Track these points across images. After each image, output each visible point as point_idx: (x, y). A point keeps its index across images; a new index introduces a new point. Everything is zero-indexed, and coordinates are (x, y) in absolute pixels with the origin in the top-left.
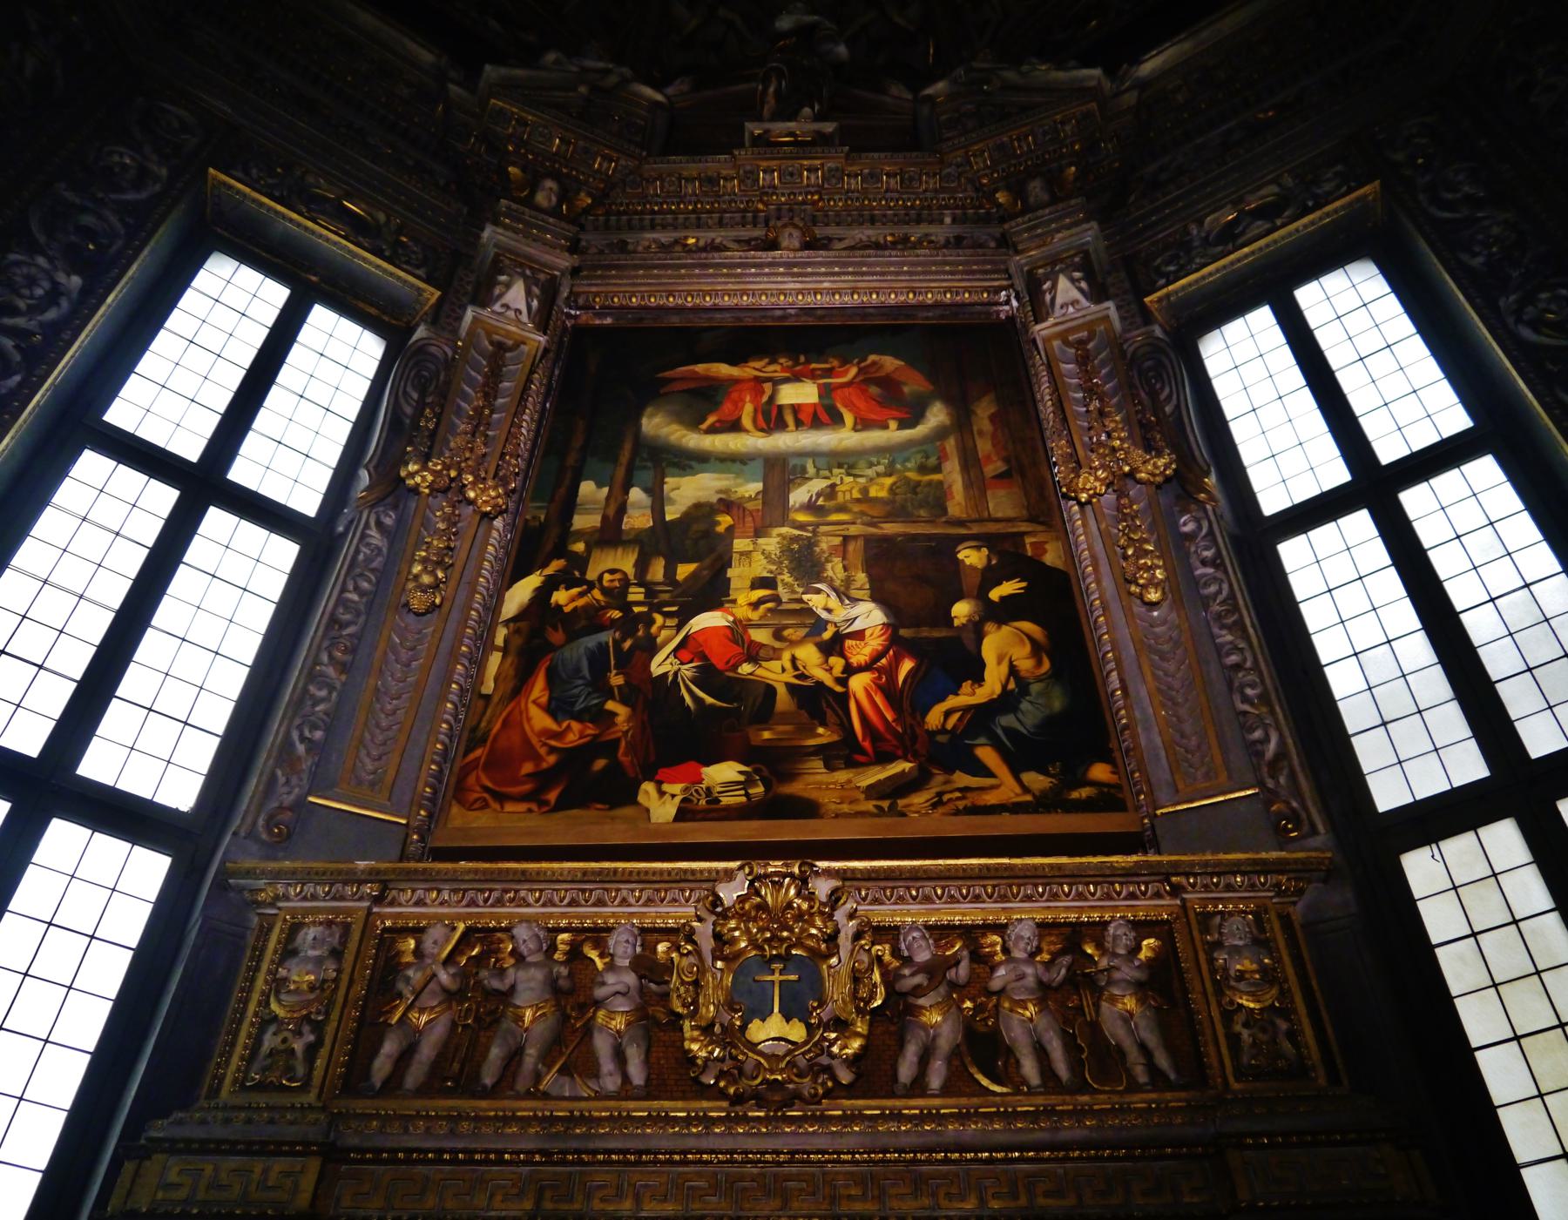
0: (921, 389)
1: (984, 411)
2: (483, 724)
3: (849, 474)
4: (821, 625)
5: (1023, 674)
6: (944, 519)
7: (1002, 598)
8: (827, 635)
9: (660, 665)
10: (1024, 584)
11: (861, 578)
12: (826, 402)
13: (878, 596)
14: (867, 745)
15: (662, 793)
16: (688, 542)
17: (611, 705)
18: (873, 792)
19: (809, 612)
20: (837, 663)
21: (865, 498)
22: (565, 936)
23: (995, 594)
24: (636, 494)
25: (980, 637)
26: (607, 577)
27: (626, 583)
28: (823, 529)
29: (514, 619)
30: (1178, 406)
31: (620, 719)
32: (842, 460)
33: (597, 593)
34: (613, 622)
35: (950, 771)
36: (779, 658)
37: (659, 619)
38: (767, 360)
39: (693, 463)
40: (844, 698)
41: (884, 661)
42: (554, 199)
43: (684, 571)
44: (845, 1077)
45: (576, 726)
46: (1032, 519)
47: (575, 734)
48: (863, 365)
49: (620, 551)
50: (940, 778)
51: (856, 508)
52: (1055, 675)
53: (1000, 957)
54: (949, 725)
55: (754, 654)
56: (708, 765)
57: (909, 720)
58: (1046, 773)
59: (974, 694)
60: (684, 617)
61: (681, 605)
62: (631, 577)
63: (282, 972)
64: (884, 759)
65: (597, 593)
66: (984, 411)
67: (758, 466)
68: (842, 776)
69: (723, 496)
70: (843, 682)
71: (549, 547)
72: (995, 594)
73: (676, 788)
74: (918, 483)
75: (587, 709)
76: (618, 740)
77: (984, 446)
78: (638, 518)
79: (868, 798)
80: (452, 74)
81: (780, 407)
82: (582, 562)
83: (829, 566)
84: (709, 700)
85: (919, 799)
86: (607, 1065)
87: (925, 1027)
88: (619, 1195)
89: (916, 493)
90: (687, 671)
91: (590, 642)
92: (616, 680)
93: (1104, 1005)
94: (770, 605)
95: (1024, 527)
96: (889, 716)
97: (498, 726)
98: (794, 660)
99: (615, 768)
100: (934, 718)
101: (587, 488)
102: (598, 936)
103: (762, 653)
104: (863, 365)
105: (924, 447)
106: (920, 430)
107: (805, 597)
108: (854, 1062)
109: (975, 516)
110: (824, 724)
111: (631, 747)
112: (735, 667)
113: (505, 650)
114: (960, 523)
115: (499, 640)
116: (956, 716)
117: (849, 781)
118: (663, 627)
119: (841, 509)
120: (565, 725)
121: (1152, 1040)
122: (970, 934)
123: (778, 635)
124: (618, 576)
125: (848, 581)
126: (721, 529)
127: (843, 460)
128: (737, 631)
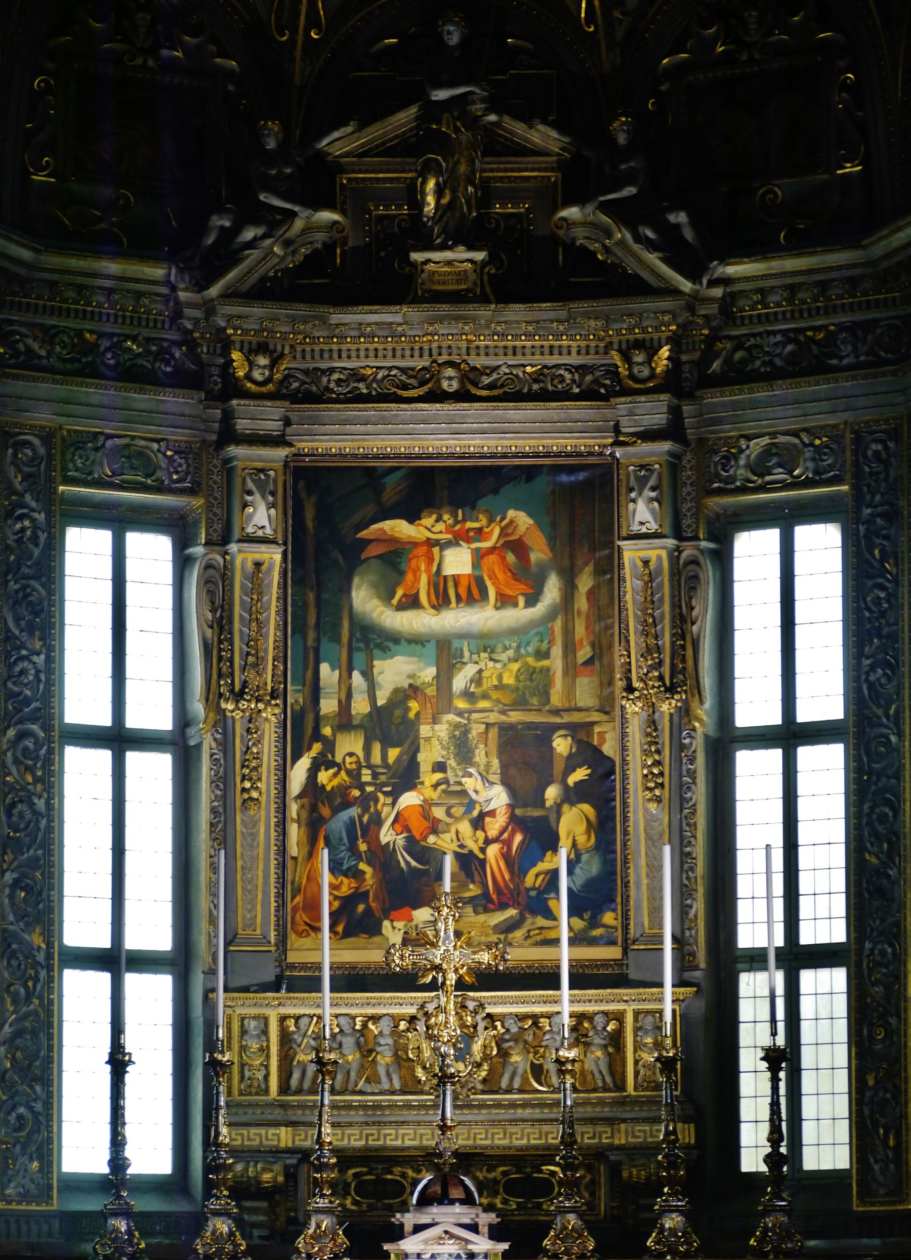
0: (543, 556)
1: (585, 583)
2: (297, 879)
3: (491, 659)
4: (471, 804)
5: (580, 846)
6: (547, 708)
7: (576, 783)
8: (475, 813)
9: (386, 835)
10: (589, 771)
11: (496, 762)
12: (477, 573)
13: (506, 782)
14: (494, 897)
15: (394, 928)
16: (393, 727)
17: (362, 866)
18: (498, 929)
19: (464, 793)
20: (480, 834)
21: (500, 687)
22: (360, 1019)
23: (572, 779)
24: (356, 675)
25: (559, 815)
26: (348, 760)
27: (360, 767)
28: (475, 716)
29: (299, 797)
30: (700, 627)
31: (368, 876)
32: (486, 642)
33: (343, 773)
34: (356, 798)
35: (534, 913)
36: (449, 832)
37: (380, 795)
38: (434, 517)
39: (390, 645)
40: (483, 862)
41: (506, 835)
42: (267, 373)
43: (393, 754)
44: (480, 1087)
45: (345, 881)
46: (601, 710)
47: (347, 886)
48: (504, 523)
49: (353, 733)
50: (529, 921)
51: (495, 695)
52: (597, 848)
53: (548, 1028)
54: (537, 885)
55: (435, 828)
56: (415, 908)
57: (517, 880)
58: (581, 918)
59: (551, 861)
60: (395, 795)
61: (394, 786)
62: (362, 760)
63: (244, 1043)
64: (502, 907)
65: (343, 773)
66: (585, 583)
67: (431, 648)
68: (482, 918)
69: (411, 681)
70: (483, 850)
71: (309, 731)
72: (572, 779)
73: (400, 925)
74: (534, 668)
75: (349, 869)
76: (368, 891)
77: (580, 629)
78: (360, 706)
79: (494, 933)
80: (182, 286)
81: (445, 577)
82: (329, 745)
83: (477, 752)
84: (414, 863)
85: (519, 934)
86: (384, 1079)
87: (512, 1064)
88: (396, 1139)
89: (531, 680)
90: (400, 841)
91: (345, 815)
92: (363, 847)
93: (588, 1054)
94: (443, 787)
95: (595, 717)
96: (507, 877)
97: (304, 881)
98: (457, 832)
99: (368, 910)
101: (325, 668)
102: (375, 1019)
103: (441, 827)
104: (504, 523)
105: (541, 629)
106: (540, 608)
107: (464, 780)
108: (484, 1081)
109: (567, 705)
110: (473, 882)
111: (376, 896)
112: (425, 839)
113: (298, 821)
114: (557, 712)
115: (294, 815)
116: (541, 878)
117: (485, 922)
118: (384, 804)
119: (485, 696)
120: (340, 880)
121: (605, 1071)
122: (535, 1018)
123: (448, 814)
124: (354, 759)
125: (488, 766)
126: (412, 715)
128: (426, 807)
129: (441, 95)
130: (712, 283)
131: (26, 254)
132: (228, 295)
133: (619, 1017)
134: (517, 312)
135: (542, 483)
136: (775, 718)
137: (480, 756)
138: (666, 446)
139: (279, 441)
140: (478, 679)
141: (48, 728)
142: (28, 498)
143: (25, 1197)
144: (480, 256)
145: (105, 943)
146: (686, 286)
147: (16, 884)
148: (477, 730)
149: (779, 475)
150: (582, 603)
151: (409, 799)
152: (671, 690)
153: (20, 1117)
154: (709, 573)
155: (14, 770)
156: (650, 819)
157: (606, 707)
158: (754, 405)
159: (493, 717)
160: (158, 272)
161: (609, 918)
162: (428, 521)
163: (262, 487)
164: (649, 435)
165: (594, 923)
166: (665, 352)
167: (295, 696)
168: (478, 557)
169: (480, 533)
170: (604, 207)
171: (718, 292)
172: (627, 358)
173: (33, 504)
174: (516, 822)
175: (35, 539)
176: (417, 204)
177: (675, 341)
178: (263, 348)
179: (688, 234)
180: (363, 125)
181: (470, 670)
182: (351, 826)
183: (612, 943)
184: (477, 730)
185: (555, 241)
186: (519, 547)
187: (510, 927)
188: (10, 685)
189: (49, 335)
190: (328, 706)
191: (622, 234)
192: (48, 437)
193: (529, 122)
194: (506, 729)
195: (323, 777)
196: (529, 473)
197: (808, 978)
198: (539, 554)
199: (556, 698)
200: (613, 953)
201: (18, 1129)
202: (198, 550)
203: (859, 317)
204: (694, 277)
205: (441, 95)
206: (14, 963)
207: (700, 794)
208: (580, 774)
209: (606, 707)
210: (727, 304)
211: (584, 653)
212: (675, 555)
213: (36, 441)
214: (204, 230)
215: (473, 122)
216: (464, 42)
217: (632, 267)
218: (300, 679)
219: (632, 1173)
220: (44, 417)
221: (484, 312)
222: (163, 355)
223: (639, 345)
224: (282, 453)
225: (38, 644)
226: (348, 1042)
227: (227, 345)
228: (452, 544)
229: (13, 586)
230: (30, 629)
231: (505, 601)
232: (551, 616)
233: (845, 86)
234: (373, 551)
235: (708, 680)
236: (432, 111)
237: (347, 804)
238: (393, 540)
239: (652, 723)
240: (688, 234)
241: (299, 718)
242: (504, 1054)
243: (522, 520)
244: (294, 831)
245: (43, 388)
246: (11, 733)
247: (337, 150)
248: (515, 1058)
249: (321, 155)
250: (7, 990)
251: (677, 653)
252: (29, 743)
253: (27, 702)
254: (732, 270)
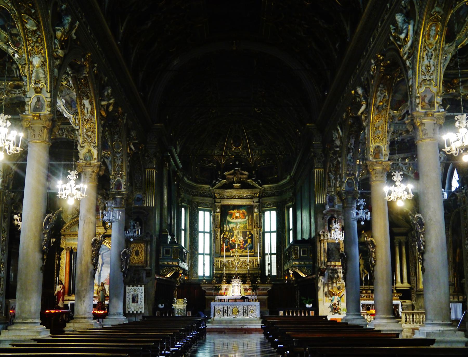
1: (250, 217)
9: (231, 242)
13: (242, 237)
43: (231, 234)
47: (227, 247)
55: (235, 241)
60: (231, 238)
66: (250, 217)
77: (250, 221)
78: (228, 229)
82: (225, 233)
100: (245, 246)
106: (246, 219)
127: (240, 223)
128: (234, 239)
129: (236, 169)
130: (263, 187)
131: (195, 184)
132: (215, 188)
133: (254, 260)
134: (244, 190)
135: (246, 207)
136: (269, 230)
137: (240, 234)
138: (258, 203)
139: (220, 203)
140: (240, 226)
141: (197, 231)
143: (195, 278)
144: (240, 184)
145: (203, 253)
146: (260, 187)
147: (194, 247)
148: (240, 231)
149: (269, 206)
150: (250, 219)
151: (233, 238)
152: (259, 227)
154: (262, 216)
156: (257, 240)
157: (252, 229)
158: (267, 199)
159: (241, 230)
160: (208, 186)
161: (253, 250)
162: (235, 211)
163: (219, 208)
164: (257, 202)
165: (251, 251)
166: (258, 194)
167: (222, 228)
168: (240, 214)
169: (240, 212)
170: (252, 180)
171: (263, 188)
172: (254, 194)
174: (243, 240)
176: (234, 179)
177: (259, 193)
178: (218, 194)
179: (260, 182)
180: (228, 172)
181: (239, 226)
182: (227, 241)
183: (253, 252)
184: (240, 231)
185: (247, 183)
186: (244, 213)
187: (243, 251)
189: (197, 192)
190: (225, 229)
191: (254, 182)
192: (197, 202)
193: (244, 171)
194: (242, 232)
195: (224, 236)
196: (245, 206)
197: (272, 256)
198: (246, 214)
199: (247, 228)
200: (253, 254)
202: (212, 214)
203: (277, 190)
204: (261, 186)
205: (236, 169)
207: (262, 238)
208: (250, 236)
209: (252, 229)
210: (264, 189)
211: (250, 224)
212: (259, 214)
214: (213, 182)
215: (239, 171)
216: (238, 163)
217: (255, 186)
218: (222, 226)
219: (255, 276)
220: (197, 200)
221: (240, 190)
222: (209, 194)
223: (255, 193)
224: (220, 204)
226: (227, 262)
227: (215, 193)
228: (237, 213)
231: (242, 219)
232: (247, 220)
233: (276, 168)
234: (229, 214)
235: (262, 227)
236: (235, 170)
237: (227, 239)
238: (231, 213)
239: (257, 231)
240: (260, 182)
241: (222, 230)
242: (242, 264)
243: (244, 211)
244: (221, 241)
245: (197, 198)
247: (226, 174)
248: (243, 264)
249: (224, 175)
251: (259, 224)
254: (265, 186)
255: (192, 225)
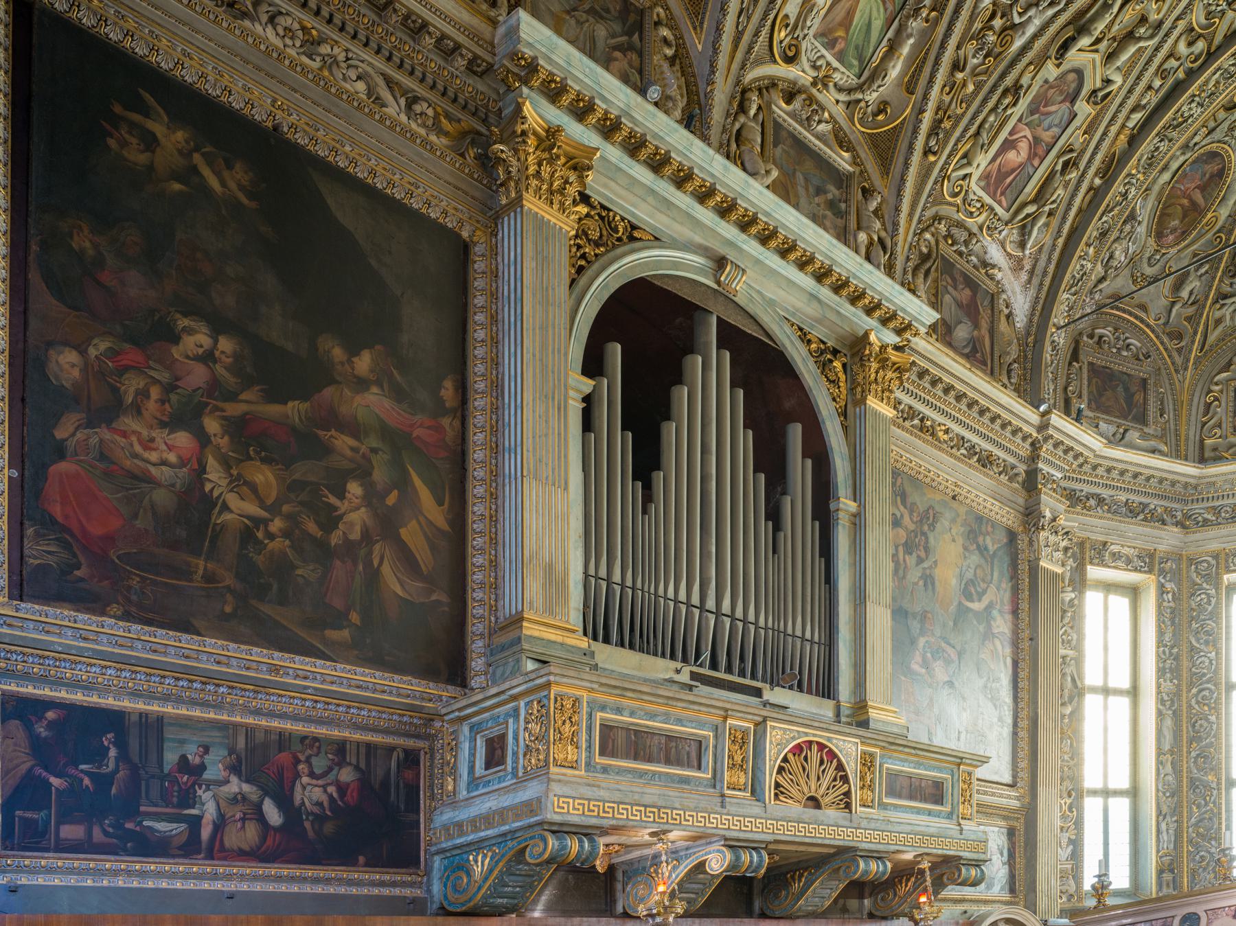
142: (1205, 585)
153: (1201, 857)
155: (1196, 706)
173: (1208, 587)
175: (1209, 603)
188: (1193, 670)
201: (1203, 861)
206: (1197, 790)
213: (1209, 559)
220: (1215, 546)
225: (1211, 649)
229: (1194, 626)
230: (1207, 643)
246: (1194, 691)
250: (1194, 803)
252: (1206, 693)
253: (1204, 675)
255: (1185, 663)
